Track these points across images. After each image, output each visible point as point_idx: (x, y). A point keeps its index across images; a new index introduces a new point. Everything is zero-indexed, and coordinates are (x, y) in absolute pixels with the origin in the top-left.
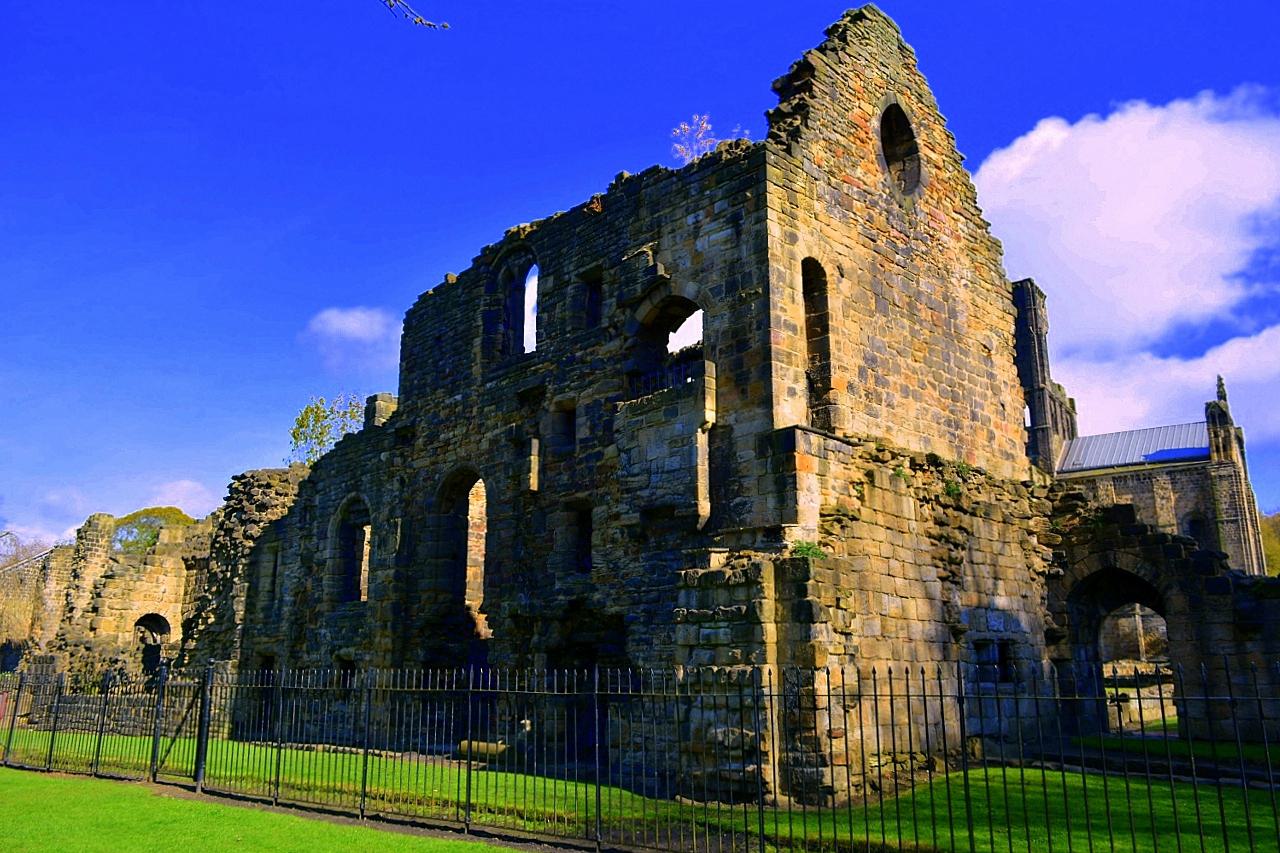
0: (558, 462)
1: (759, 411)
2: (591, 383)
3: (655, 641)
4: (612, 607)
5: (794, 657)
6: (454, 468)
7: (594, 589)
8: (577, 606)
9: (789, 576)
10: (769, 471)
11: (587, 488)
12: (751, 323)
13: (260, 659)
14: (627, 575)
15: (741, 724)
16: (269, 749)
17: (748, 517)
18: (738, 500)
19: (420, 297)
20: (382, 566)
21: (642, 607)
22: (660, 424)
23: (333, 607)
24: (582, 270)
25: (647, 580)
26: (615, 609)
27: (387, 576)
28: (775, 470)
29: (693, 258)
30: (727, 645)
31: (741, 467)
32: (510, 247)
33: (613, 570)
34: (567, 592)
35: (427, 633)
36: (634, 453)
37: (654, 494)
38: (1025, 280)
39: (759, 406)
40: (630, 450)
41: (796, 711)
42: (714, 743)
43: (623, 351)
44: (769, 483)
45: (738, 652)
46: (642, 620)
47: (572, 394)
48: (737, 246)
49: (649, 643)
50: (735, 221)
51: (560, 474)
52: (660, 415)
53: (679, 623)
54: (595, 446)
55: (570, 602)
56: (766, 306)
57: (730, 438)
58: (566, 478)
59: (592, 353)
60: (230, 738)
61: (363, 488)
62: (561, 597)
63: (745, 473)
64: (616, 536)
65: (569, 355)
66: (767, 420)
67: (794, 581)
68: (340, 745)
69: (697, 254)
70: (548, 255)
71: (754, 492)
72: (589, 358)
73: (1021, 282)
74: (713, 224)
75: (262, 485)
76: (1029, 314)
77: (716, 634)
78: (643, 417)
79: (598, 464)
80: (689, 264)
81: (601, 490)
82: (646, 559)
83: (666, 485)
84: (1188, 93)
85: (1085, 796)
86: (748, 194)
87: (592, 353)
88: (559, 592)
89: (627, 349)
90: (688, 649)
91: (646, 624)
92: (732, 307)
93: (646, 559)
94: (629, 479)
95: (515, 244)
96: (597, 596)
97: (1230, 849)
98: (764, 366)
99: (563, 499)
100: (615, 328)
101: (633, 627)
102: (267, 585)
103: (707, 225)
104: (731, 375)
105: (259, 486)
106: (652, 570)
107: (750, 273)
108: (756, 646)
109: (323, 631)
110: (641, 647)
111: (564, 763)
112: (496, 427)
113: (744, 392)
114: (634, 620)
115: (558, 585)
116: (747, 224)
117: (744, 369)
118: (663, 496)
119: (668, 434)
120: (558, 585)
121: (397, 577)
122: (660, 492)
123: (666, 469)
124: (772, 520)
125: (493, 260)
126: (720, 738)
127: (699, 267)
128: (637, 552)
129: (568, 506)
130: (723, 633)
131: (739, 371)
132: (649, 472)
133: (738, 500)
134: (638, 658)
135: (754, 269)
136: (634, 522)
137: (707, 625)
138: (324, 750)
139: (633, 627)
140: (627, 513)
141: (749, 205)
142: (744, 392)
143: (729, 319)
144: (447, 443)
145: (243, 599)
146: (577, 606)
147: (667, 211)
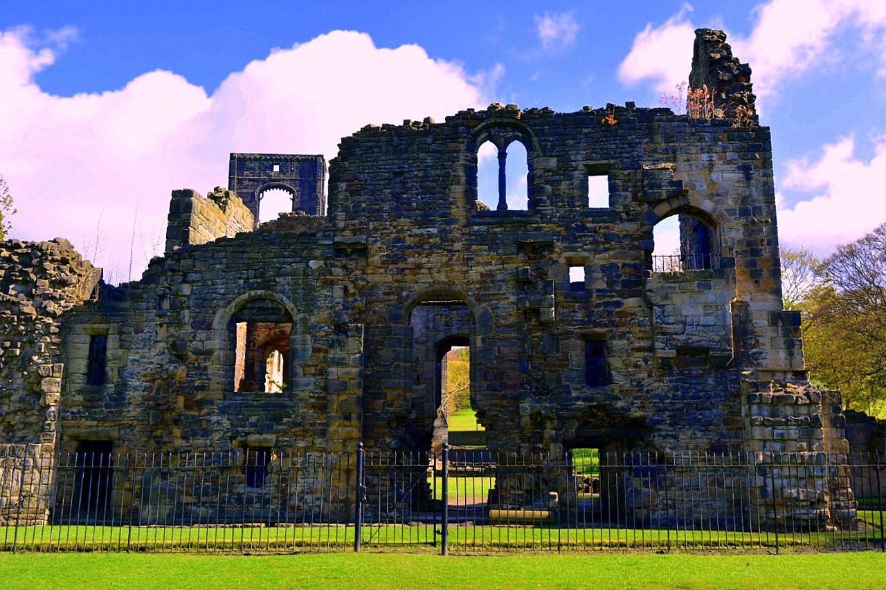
0: (574, 302)
1: (771, 297)
2: (606, 250)
3: (682, 436)
4: (636, 412)
5: (832, 448)
6: (431, 289)
7: (617, 398)
9: (827, 401)
10: (780, 335)
11: (606, 326)
12: (762, 241)
13: (74, 444)
14: (652, 391)
15: (806, 486)
17: (764, 362)
18: (755, 350)
21: (667, 413)
22: (692, 292)
23: (224, 396)
24: (591, 163)
25: (671, 395)
26: (639, 414)
28: (786, 334)
29: (709, 184)
30: (796, 440)
31: (757, 330)
32: (498, 120)
33: (637, 386)
35: (394, 425)
37: (690, 338)
38: (319, 156)
39: (771, 293)
40: (664, 306)
41: (836, 478)
42: (790, 498)
43: (639, 233)
44: (781, 342)
45: (804, 444)
46: (668, 422)
47: (585, 254)
48: (748, 186)
50: (746, 169)
51: (575, 312)
52: (694, 286)
53: (756, 425)
54: (614, 296)
55: (589, 406)
56: (774, 231)
57: (746, 309)
58: (580, 315)
59: (607, 228)
60: (50, 523)
61: (279, 288)
63: (760, 333)
64: (639, 363)
65: (578, 223)
66: (777, 304)
67: (831, 404)
69: (712, 183)
70: (550, 141)
71: (768, 347)
72: (602, 231)
73: (315, 156)
74: (726, 166)
75: (57, 260)
76: (318, 184)
77: (789, 434)
78: (676, 285)
79: (618, 310)
80: (705, 187)
81: (622, 329)
83: (701, 334)
84: (448, 59)
86: (757, 156)
87: (607, 228)
88: (578, 398)
89: (643, 232)
90: (762, 443)
92: (745, 225)
94: (664, 325)
95: (511, 120)
97: (447, 551)
98: (774, 270)
99: (579, 331)
100: (628, 214)
102: (82, 367)
103: (719, 165)
104: (747, 270)
105: (53, 261)
107: (760, 208)
108: (815, 441)
110: (667, 440)
111: (591, 521)
113: (756, 282)
115: (574, 394)
116: (756, 175)
117: (758, 268)
118: (700, 341)
119: (702, 301)
120: (574, 394)
121: (360, 374)
122: (694, 338)
123: (701, 323)
124: (783, 365)
125: (476, 126)
126: (795, 495)
127: (714, 191)
129: (583, 336)
130: (793, 432)
131: (753, 269)
132: (685, 324)
133: (755, 350)
134: (665, 447)
135: (763, 206)
136: (671, 356)
137: (780, 427)
140: (663, 349)
141: (758, 163)
143: (744, 233)
145: (59, 380)
147: (682, 144)
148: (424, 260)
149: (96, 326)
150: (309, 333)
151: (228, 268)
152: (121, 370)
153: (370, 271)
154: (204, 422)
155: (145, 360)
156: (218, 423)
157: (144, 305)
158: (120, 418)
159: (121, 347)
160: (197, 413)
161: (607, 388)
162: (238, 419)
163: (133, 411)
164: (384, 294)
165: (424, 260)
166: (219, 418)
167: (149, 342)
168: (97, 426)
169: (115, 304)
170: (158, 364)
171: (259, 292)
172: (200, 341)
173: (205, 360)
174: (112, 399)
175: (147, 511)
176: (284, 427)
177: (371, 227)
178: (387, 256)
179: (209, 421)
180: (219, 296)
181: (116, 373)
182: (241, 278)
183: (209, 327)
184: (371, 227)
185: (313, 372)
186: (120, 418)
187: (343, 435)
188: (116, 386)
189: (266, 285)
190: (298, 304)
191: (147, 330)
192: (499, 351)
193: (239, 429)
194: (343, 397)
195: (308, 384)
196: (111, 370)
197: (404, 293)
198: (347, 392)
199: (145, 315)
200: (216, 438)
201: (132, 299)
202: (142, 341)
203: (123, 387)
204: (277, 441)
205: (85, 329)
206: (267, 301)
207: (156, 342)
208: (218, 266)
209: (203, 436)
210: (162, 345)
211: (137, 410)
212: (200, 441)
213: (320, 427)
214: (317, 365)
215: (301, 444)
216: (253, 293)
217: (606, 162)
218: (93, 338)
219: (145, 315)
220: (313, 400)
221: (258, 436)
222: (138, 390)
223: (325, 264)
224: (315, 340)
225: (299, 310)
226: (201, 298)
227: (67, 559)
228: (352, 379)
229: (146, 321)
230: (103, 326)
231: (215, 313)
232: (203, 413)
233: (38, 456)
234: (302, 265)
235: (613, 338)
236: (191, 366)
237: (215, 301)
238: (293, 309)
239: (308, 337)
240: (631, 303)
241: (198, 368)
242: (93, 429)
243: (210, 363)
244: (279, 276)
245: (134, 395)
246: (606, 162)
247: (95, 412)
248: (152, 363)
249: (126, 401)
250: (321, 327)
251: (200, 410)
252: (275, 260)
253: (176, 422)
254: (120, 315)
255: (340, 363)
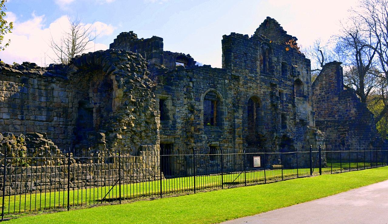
3: (298, 144)
8: (285, 136)
16: (258, 172)
19: (232, 33)
20: (237, 118)
24: (283, 61)
27: (240, 121)
34: (283, 133)
36: (298, 108)
49: (297, 144)
59: (286, 82)
62: (282, 134)
68: (232, 172)
82: (296, 128)
85: (341, 161)
87: (286, 82)
88: (281, 132)
91: (296, 141)
93: (296, 128)
96: (288, 134)
101: (294, 141)
106: (297, 131)
109: (203, 136)
112: (265, 89)
113: (309, 103)
114: (294, 140)
122: (302, 117)
128: (295, 127)
138: (250, 172)
139: (294, 141)
142: (309, 103)
144: (251, 87)
146: (285, 136)
148: (252, 85)
149: (164, 96)
150: (227, 106)
151: (204, 79)
152: (174, 115)
153: (240, 87)
154: (200, 137)
155: (181, 112)
156: (204, 137)
157: (180, 89)
158: (175, 135)
159: (173, 105)
160: (198, 134)
161: (286, 129)
162: (209, 136)
163: (179, 132)
164: (244, 95)
165: (252, 85)
166: (205, 136)
167: (182, 105)
168: (167, 138)
169: (170, 87)
170: (186, 114)
171: (213, 89)
172: (197, 106)
173: (199, 113)
174: (172, 127)
175: (190, 171)
176: (222, 139)
177: (240, 71)
178: (243, 82)
179: (201, 137)
180: (202, 89)
181: (172, 116)
182: (207, 83)
183: (199, 101)
184: (240, 71)
185: (228, 120)
186: (175, 135)
187: (239, 142)
188: (172, 122)
189: (215, 87)
190: (223, 95)
191: (181, 99)
192: (267, 117)
193: (210, 140)
194: (239, 130)
195: (227, 124)
196: (170, 114)
197: (248, 95)
198: (240, 128)
199: (180, 93)
200: (204, 143)
201: (175, 86)
202: (179, 104)
203: (175, 122)
204: (220, 144)
205: (160, 96)
206: (213, 93)
207: (184, 105)
208: (201, 77)
209: (200, 142)
210: (186, 106)
211: (180, 131)
212: (199, 144)
213: (230, 140)
214: (229, 118)
215: (226, 145)
216: (211, 89)
217: (285, 62)
218: (160, 100)
219: (180, 93)
220: (228, 130)
221: (214, 142)
222: (180, 124)
223: (229, 82)
224: (228, 109)
225: (223, 98)
226: (196, 89)
227: (366, 171)
228: (240, 123)
229: (181, 96)
230: (166, 96)
231: (201, 95)
232: (199, 134)
233: (156, 150)
234: (223, 81)
235: (287, 115)
236: (195, 115)
237: (201, 91)
238: (222, 97)
239: (226, 107)
240: (290, 105)
241: (197, 116)
242: (166, 139)
243: (201, 115)
244: (218, 84)
245: (179, 126)
246: (285, 62)
247: (166, 132)
248: (184, 113)
249: (176, 128)
250: (230, 105)
251: (199, 132)
252: (216, 78)
253: (192, 137)
254: (172, 92)
255: (238, 118)
